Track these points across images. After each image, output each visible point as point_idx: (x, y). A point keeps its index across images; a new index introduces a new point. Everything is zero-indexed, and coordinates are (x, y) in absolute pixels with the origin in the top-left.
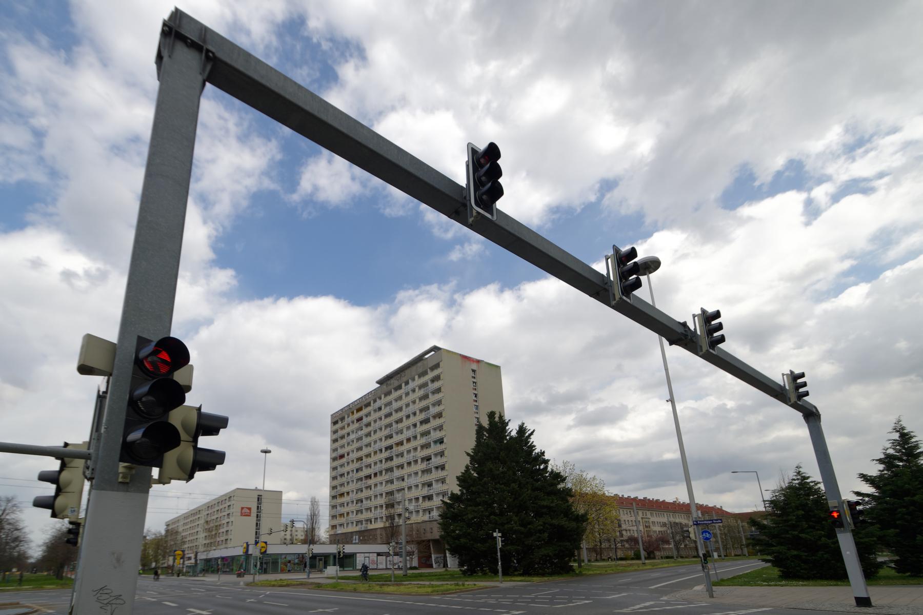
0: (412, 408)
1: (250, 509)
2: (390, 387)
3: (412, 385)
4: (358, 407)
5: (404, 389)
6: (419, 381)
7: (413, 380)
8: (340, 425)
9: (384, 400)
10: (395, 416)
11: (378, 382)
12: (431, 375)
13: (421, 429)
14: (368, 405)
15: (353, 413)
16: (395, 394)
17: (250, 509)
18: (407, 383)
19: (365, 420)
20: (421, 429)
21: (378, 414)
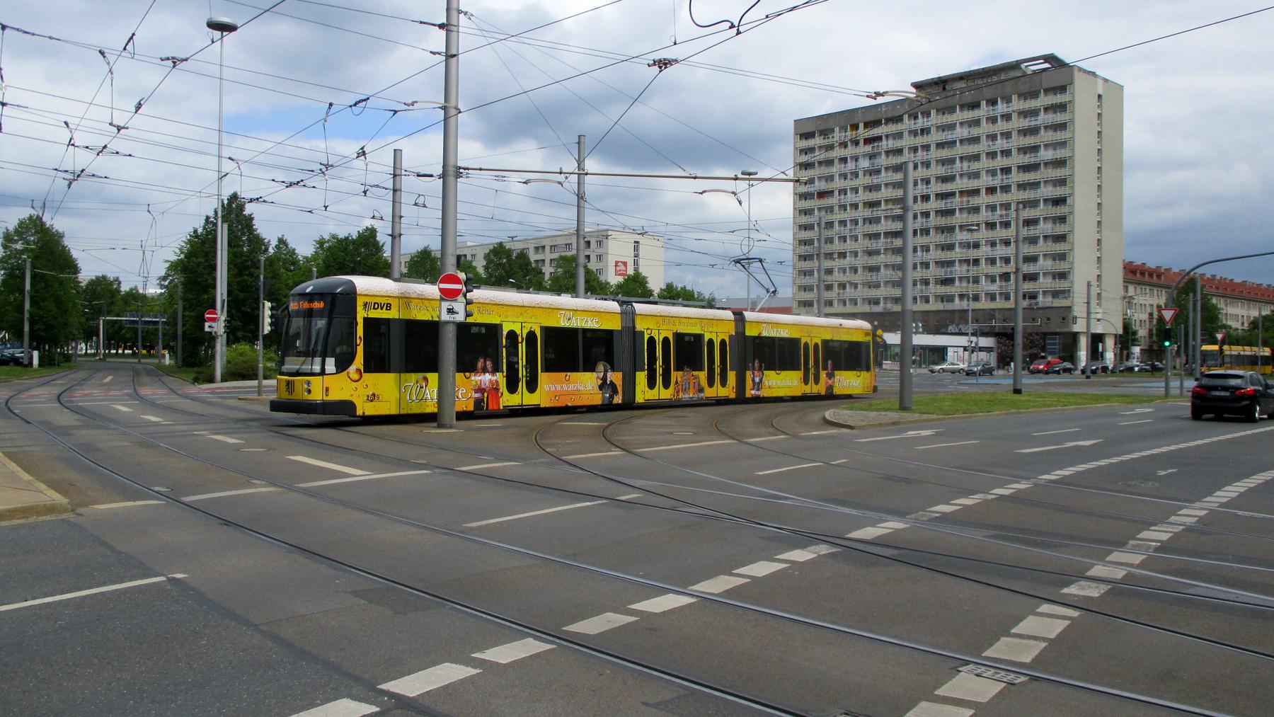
0: (1000, 144)
1: (625, 264)
2: (950, 102)
3: (1001, 108)
4: (871, 118)
5: (984, 111)
6: (1017, 104)
7: (1008, 100)
8: (817, 141)
9: (935, 119)
10: (960, 150)
11: (918, 86)
12: (1044, 100)
13: (1016, 177)
14: (898, 119)
15: (855, 127)
16: (960, 115)
17: (625, 264)
18: (993, 102)
19: (886, 144)
20: (1016, 177)
21: (920, 141)
